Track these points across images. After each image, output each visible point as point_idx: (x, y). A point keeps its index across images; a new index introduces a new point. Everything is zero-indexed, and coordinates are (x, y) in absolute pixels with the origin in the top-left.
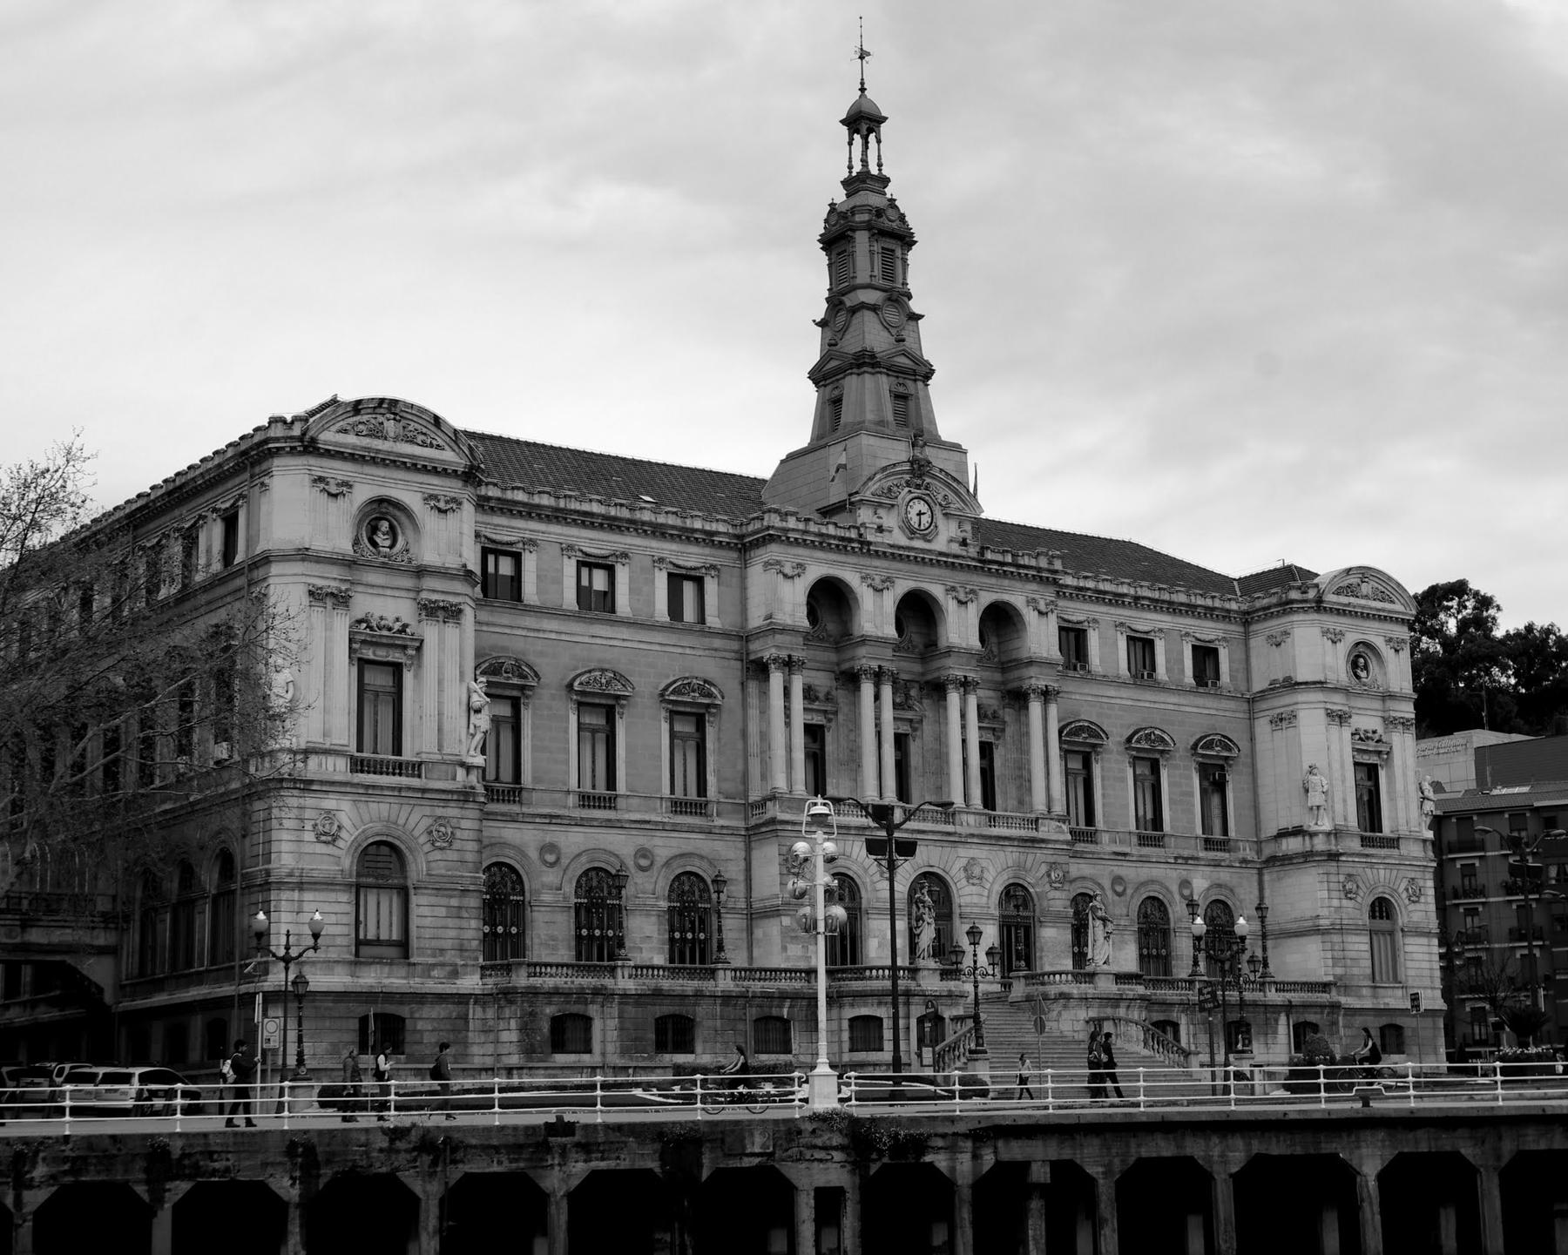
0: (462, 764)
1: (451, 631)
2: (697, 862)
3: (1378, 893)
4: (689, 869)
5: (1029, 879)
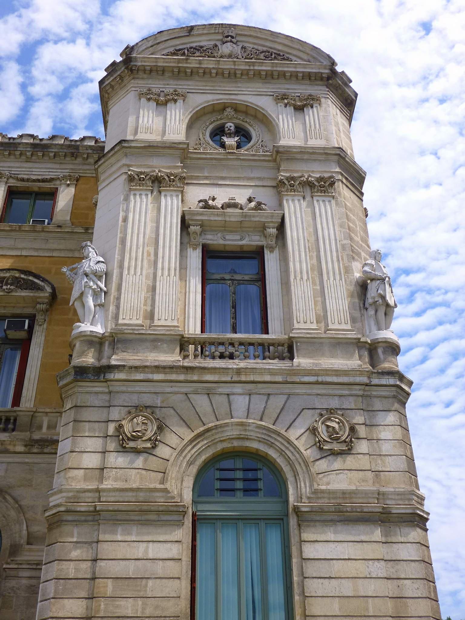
3: (229, 437)
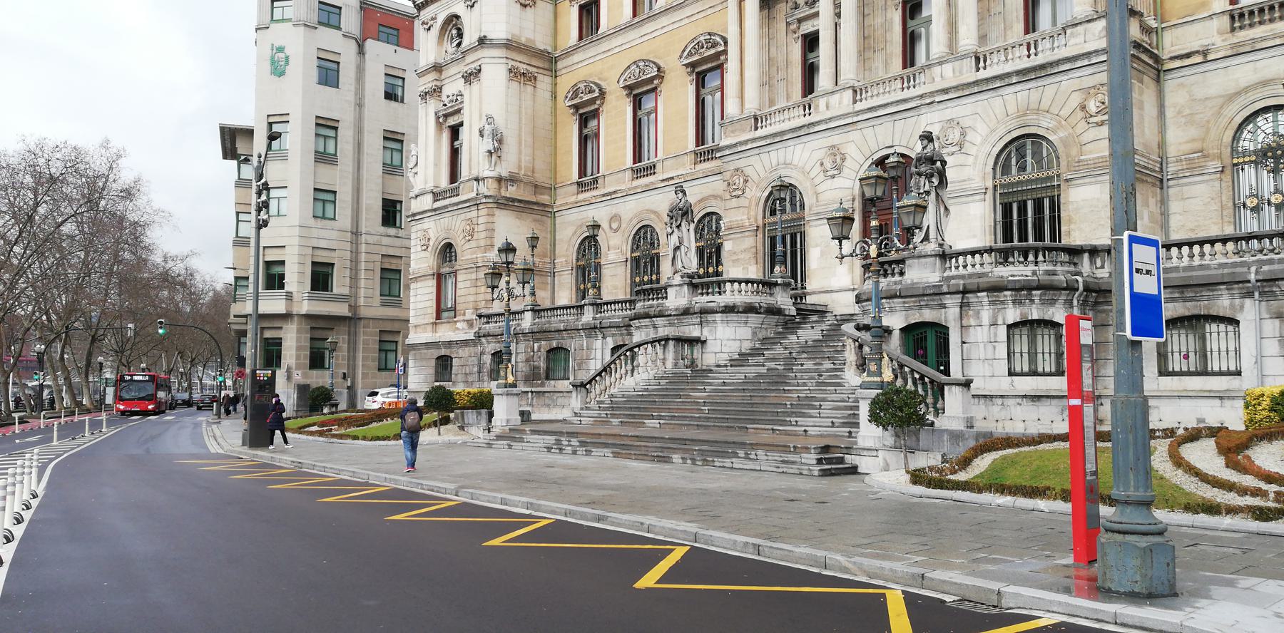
0: (477, 179)
1: (475, 86)
2: (713, 202)
4: (709, 210)
5: (1043, 125)
